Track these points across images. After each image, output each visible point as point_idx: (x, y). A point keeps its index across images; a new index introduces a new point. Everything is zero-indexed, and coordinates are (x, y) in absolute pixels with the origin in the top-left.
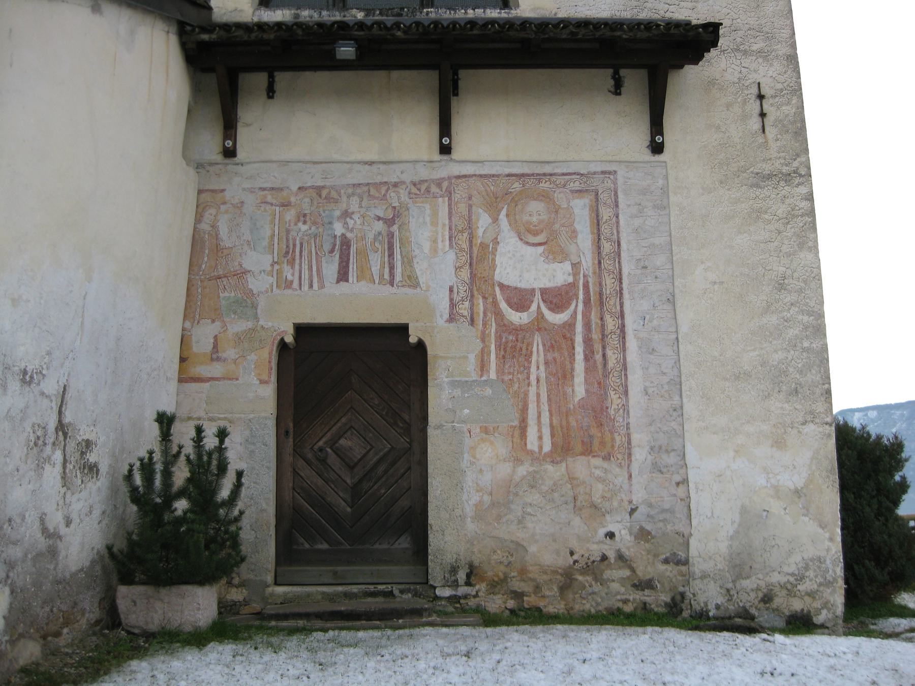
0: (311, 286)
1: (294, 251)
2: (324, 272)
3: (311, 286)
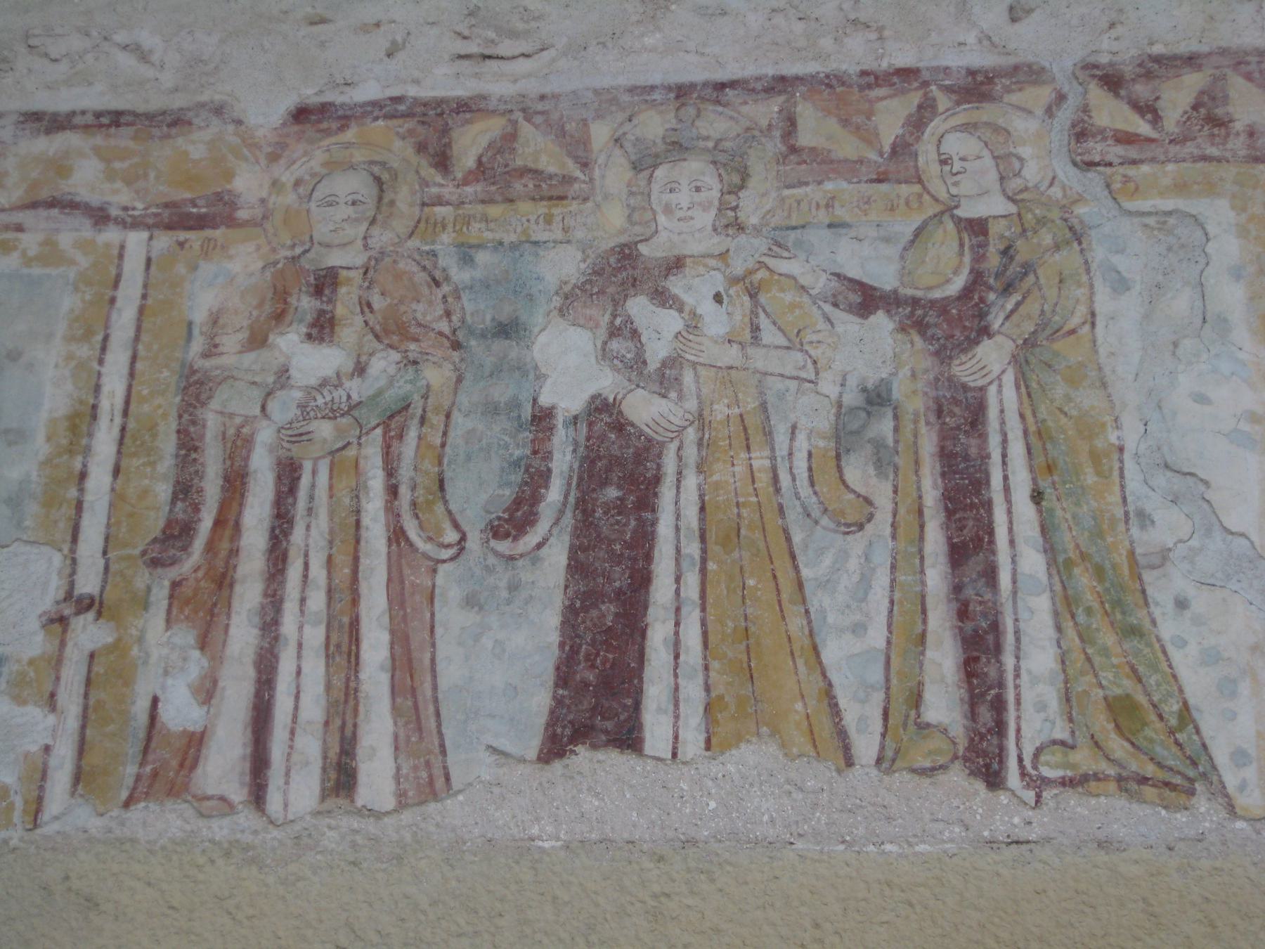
0: (342, 778)
1: (228, 522)
2: (451, 673)
3: (342, 778)
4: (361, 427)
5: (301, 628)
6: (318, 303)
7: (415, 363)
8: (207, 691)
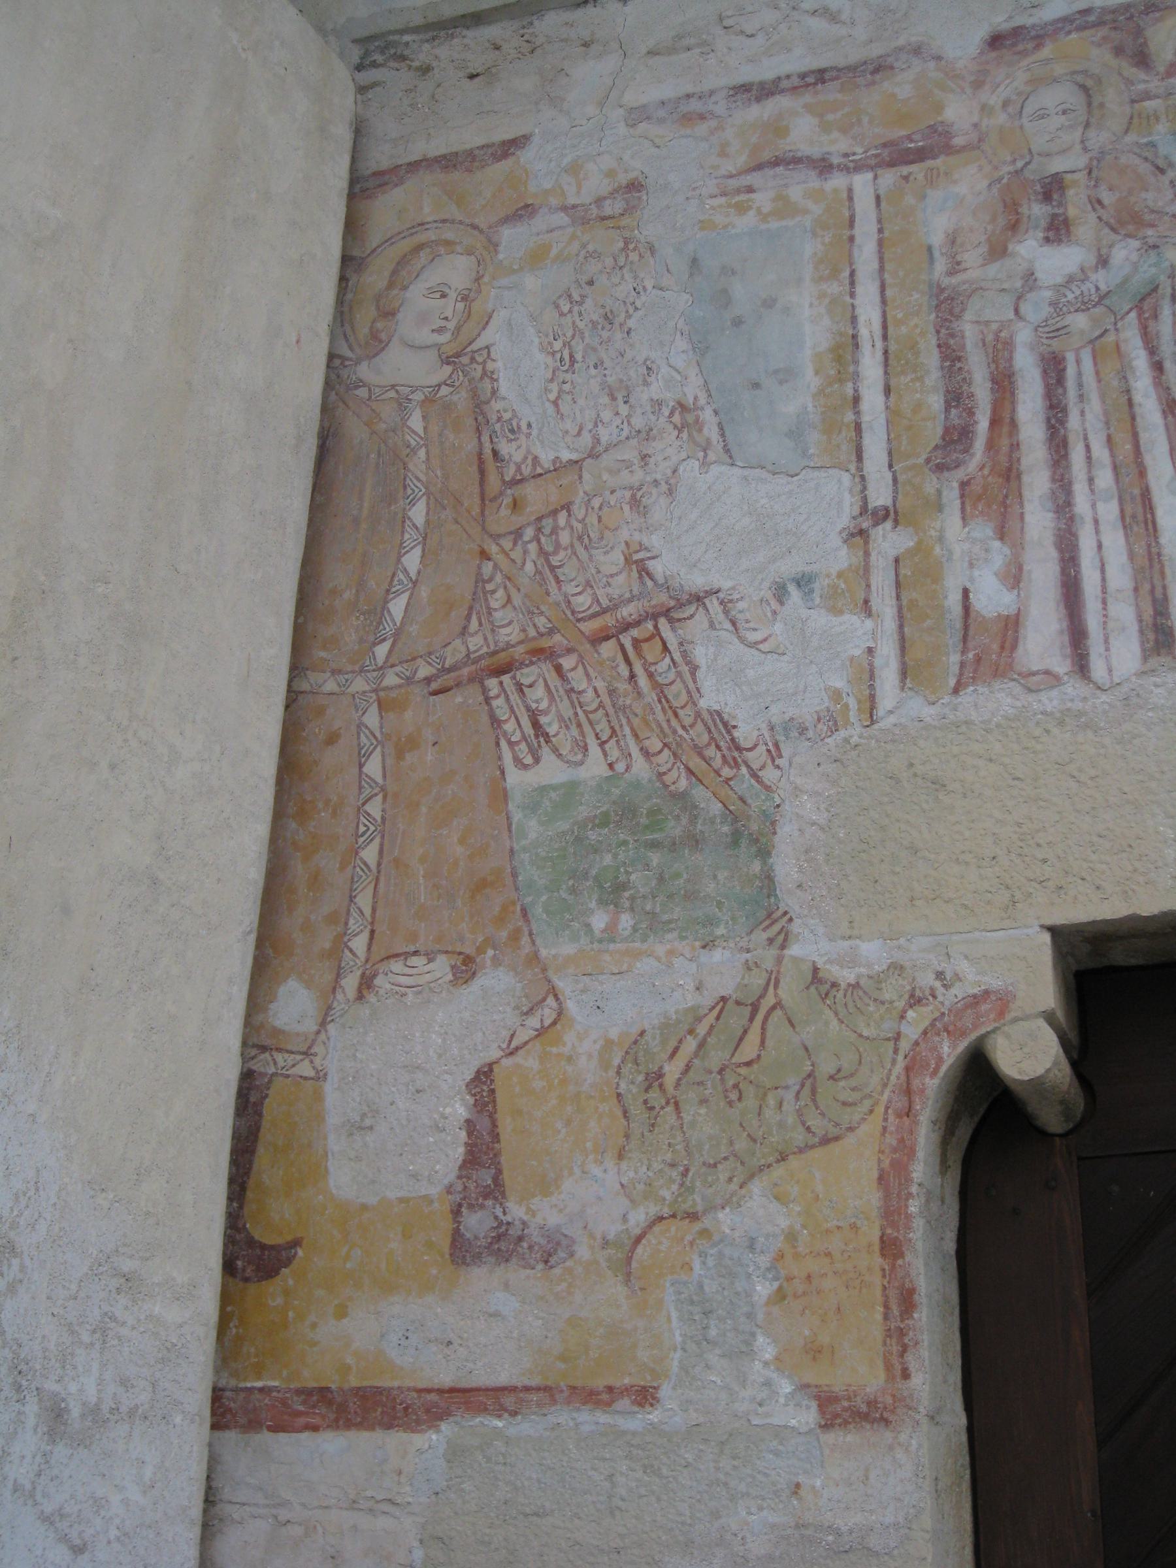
1: (1003, 420)
4: (1115, 314)
5: (1094, 506)
6: (1049, 208)
7: (1155, 247)
8: (1014, 577)
